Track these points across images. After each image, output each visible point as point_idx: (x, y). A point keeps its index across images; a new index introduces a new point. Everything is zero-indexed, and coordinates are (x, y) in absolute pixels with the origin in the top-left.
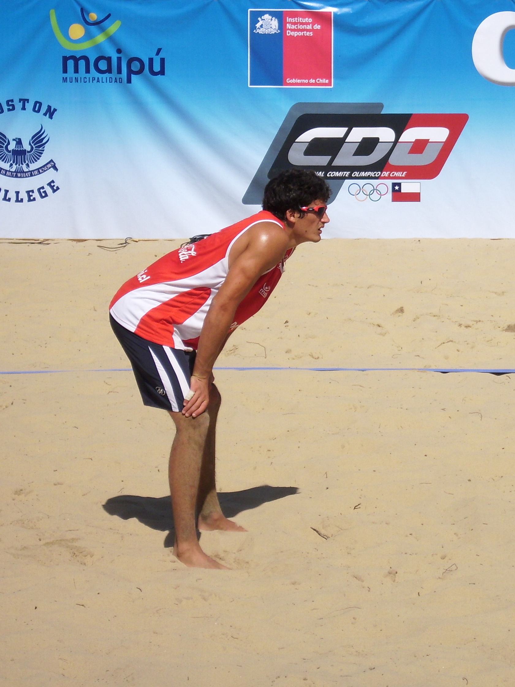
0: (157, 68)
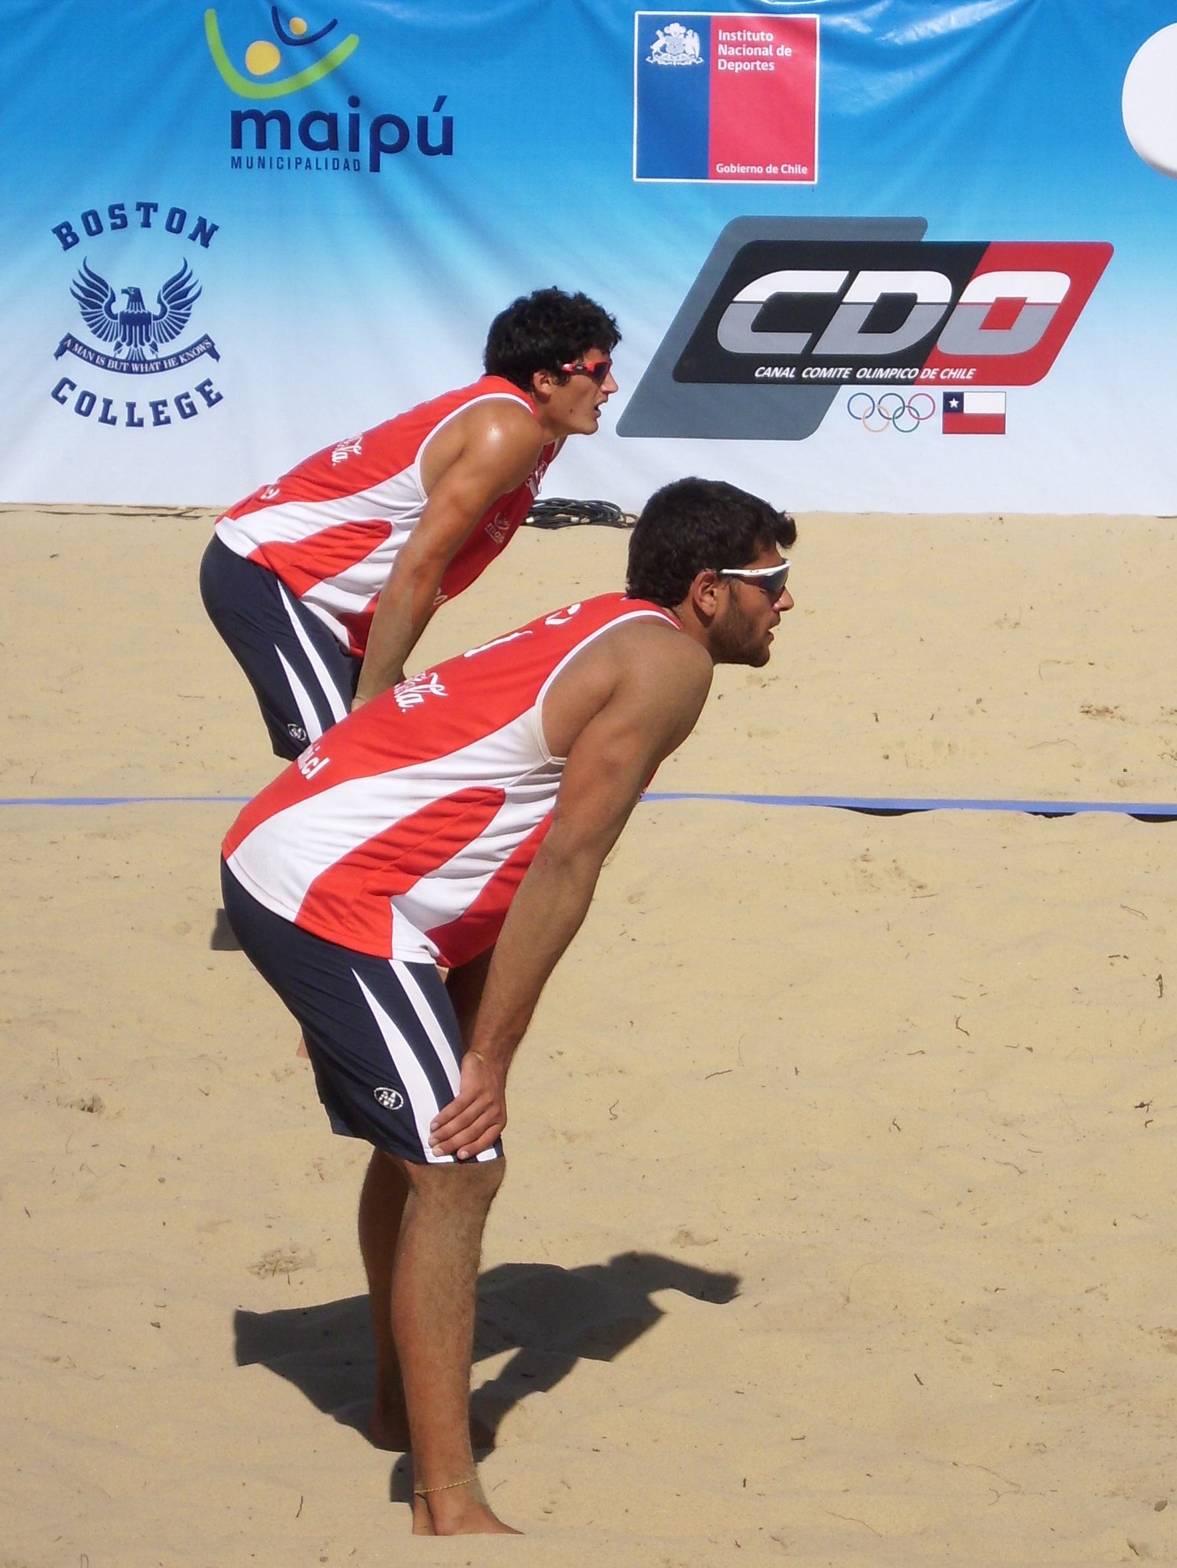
0: (435, 138)
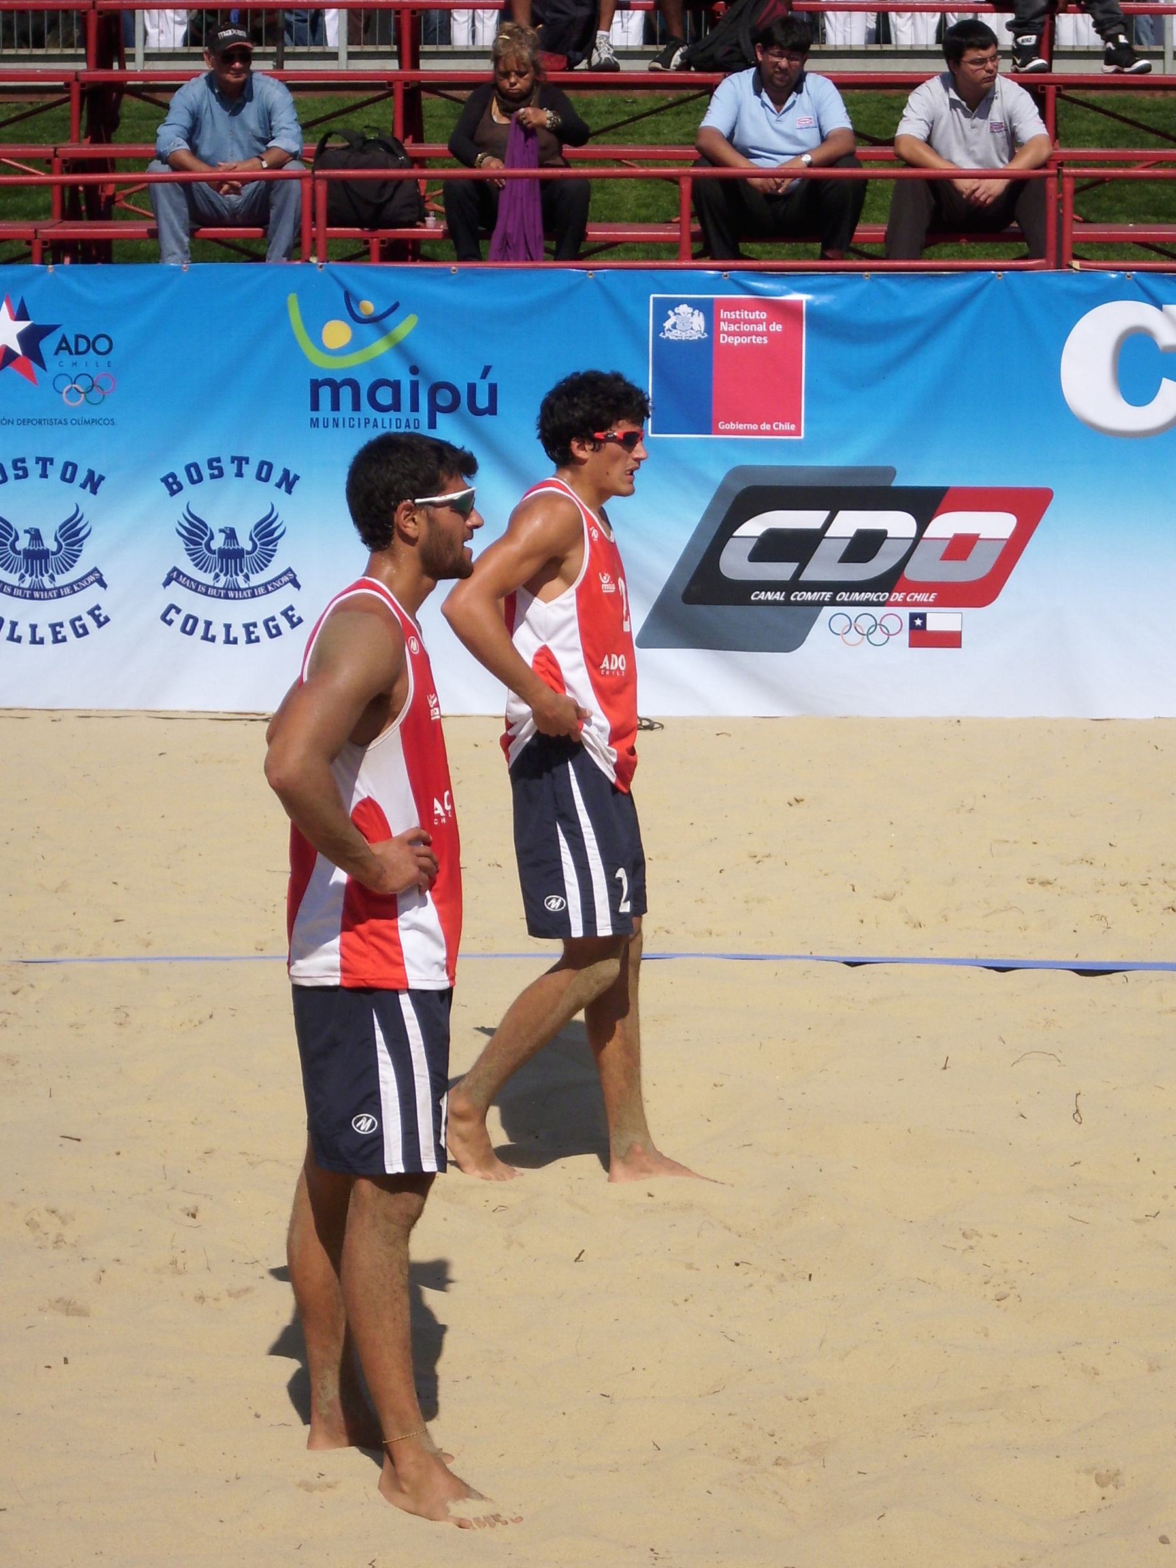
0: (482, 401)
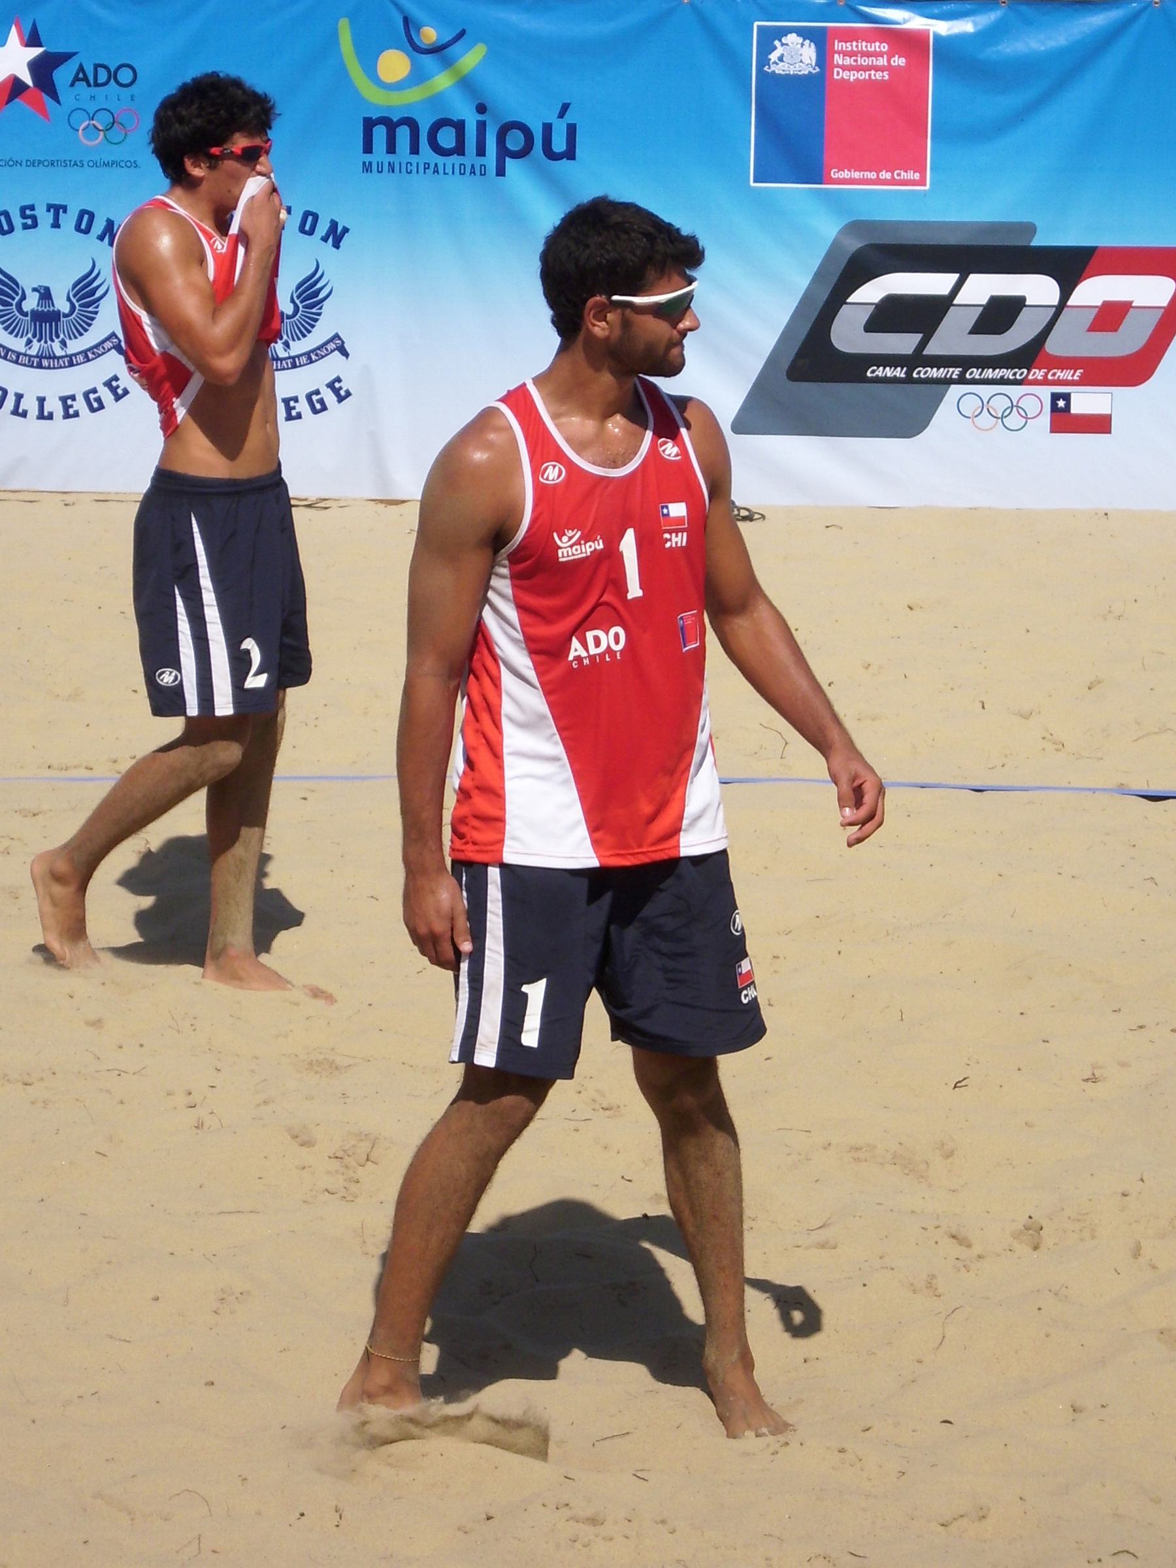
0: (559, 144)
